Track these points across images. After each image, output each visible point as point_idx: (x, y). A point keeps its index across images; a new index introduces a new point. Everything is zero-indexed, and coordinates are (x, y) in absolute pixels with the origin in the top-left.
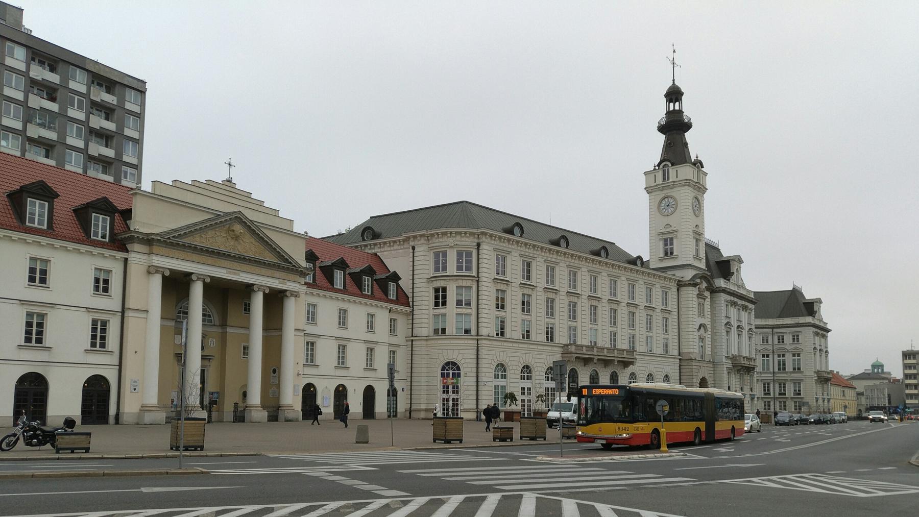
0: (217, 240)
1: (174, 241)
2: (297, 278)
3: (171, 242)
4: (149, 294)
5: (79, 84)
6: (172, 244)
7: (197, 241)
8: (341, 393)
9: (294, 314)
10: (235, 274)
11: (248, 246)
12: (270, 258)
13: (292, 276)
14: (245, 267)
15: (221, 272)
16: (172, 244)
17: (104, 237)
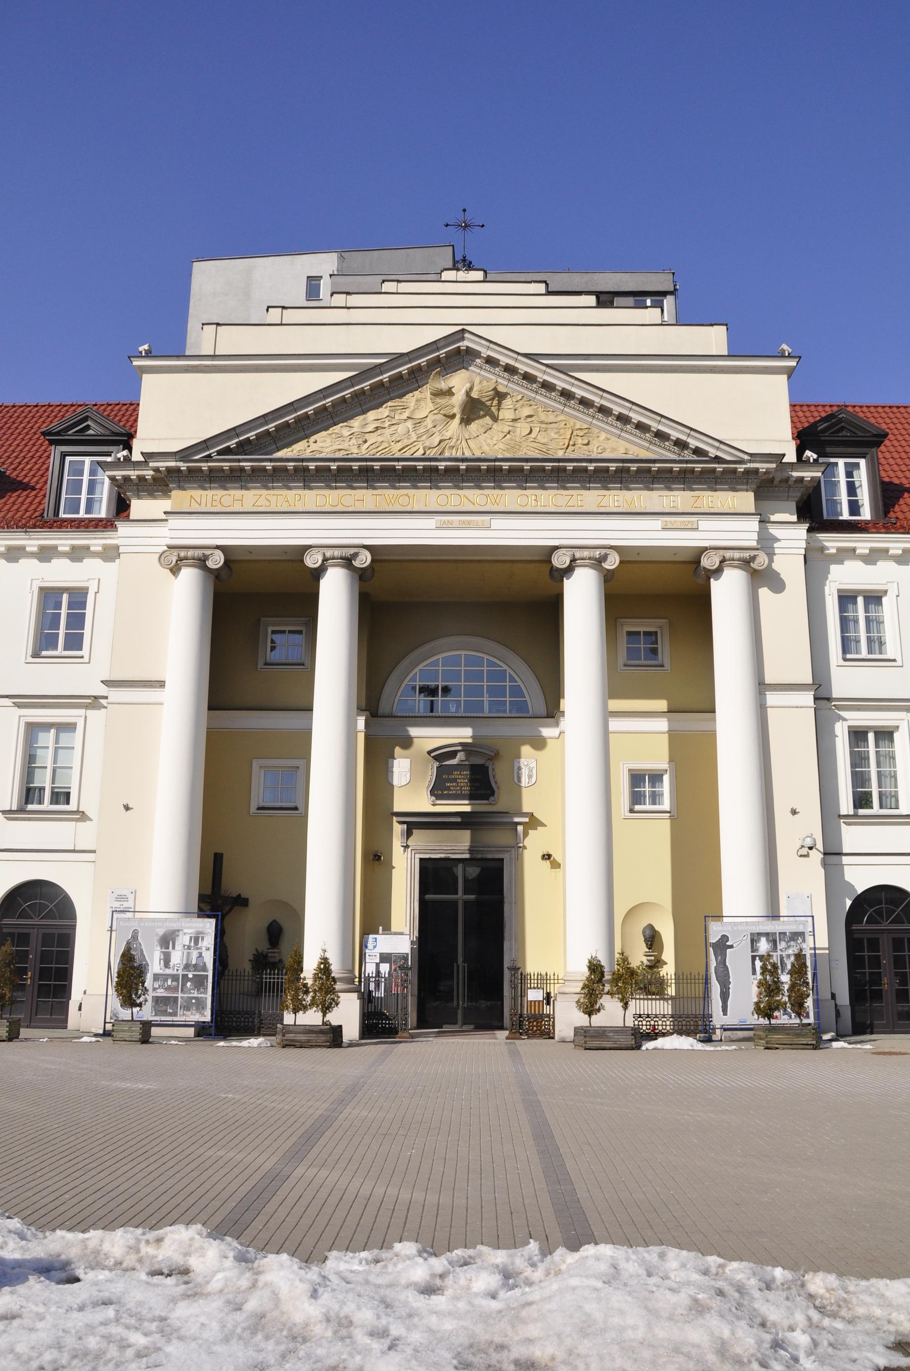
2: (745, 500)
11: (524, 429)
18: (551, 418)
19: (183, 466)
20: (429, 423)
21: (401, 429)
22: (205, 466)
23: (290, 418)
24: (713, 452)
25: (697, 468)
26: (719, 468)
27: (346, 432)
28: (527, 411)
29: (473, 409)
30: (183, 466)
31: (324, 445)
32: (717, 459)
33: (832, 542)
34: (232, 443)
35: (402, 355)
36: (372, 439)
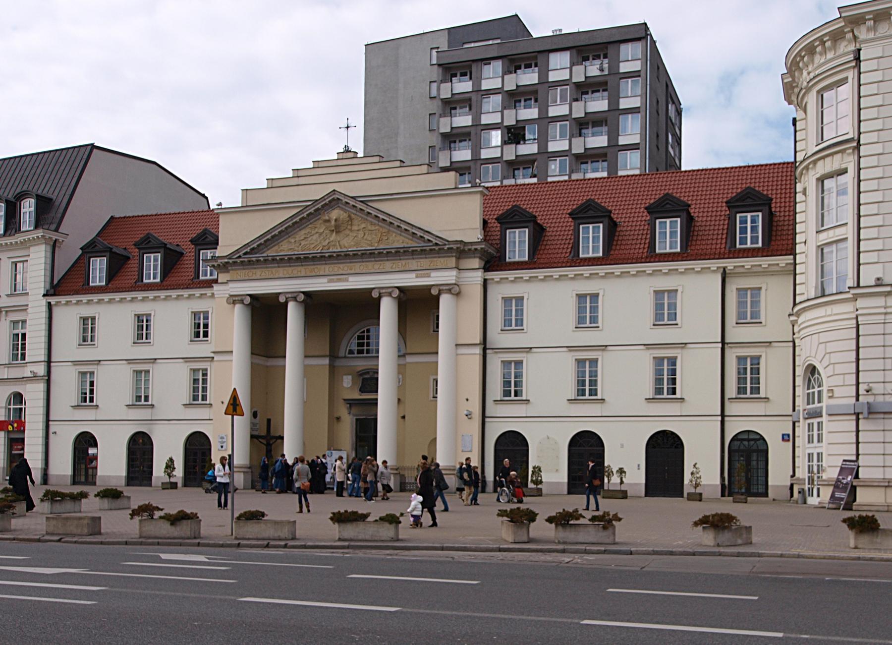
0: (312, 240)
1: (245, 259)
2: (452, 262)
3: (252, 257)
4: (232, 329)
5: (560, 66)
6: (250, 262)
7: (285, 248)
8: (586, 450)
9: (455, 320)
10: (339, 280)
12: (398, 241)
13: (441, 262)
14: (358, 267)
15: (320, 283)
16: (250, 262)
17: (754, 240)
18: (373, 228)
19: (231, 261)
20: (324, 234)
21: (315, 237)
22: (238, 260)
23: (269, 237)
24: (434, 241)
25: (432, 248)
26: (437, 248)
27: (293, 241)
28: (363, 225)
29: (337, 229)
30: (231, 261)
31: (285, 248)
32: (437, 244)
33: (495, 275)
34: (248, 250)
35: (317, 200)
36: (303, 243)
